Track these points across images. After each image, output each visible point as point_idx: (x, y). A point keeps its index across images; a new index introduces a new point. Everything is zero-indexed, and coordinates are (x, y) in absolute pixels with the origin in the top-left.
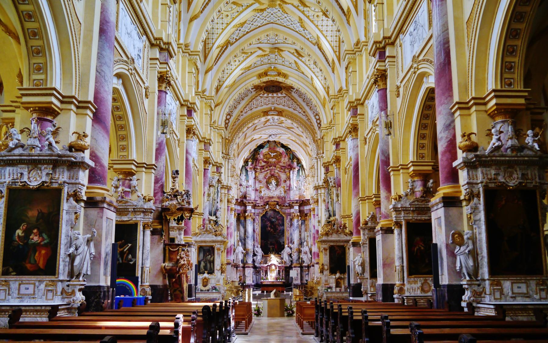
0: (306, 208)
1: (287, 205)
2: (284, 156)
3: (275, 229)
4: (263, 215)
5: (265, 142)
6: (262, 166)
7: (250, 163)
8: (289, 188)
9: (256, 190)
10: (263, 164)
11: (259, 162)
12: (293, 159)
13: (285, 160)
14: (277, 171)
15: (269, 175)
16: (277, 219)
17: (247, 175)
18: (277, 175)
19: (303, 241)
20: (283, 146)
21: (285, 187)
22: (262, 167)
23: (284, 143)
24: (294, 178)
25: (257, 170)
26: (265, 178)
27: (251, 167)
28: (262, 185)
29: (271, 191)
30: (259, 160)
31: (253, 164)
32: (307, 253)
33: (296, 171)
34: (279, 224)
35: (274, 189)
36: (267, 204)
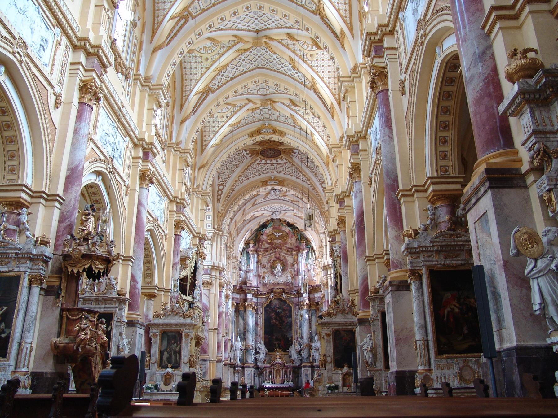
0: (317, 295)
1: (295, 292)
2: (290, 236)
3: (282, 322)
4: (267, 305)
5: (268, 220)
6: (265, 249)
7: (251, 245)
8: (298, 273)
9: (259, 276)
10: (267, 246)
11: (262, 244)
12: (301, 239)
13: (292, 241)
14: (282, 254)
15: (274, 258)
16: (284, 310)
17: (248, 259)
18: (283, 258)
19: (314, 335)
20: (289, 225)
21: (293, 273)
22: (266, 250)
23: (291, 221)
24: (303, 261)
25: (260, 253)
26: (269, 261)
27: (253, 249)
28: (265, 270)
29: (277, 277)
30: (262, 242)
31: (255, 246)
32: (318, 350)
33: (305, 253)
34: (286, 315)
35: (280, 274)
36: (272, 292)
